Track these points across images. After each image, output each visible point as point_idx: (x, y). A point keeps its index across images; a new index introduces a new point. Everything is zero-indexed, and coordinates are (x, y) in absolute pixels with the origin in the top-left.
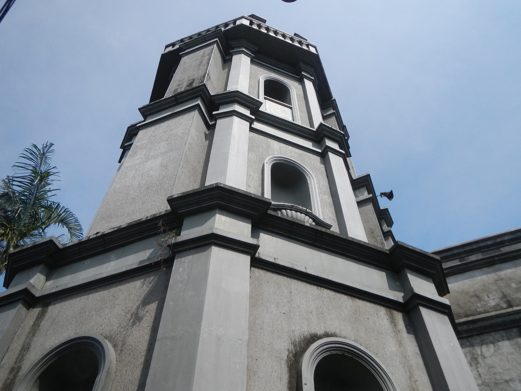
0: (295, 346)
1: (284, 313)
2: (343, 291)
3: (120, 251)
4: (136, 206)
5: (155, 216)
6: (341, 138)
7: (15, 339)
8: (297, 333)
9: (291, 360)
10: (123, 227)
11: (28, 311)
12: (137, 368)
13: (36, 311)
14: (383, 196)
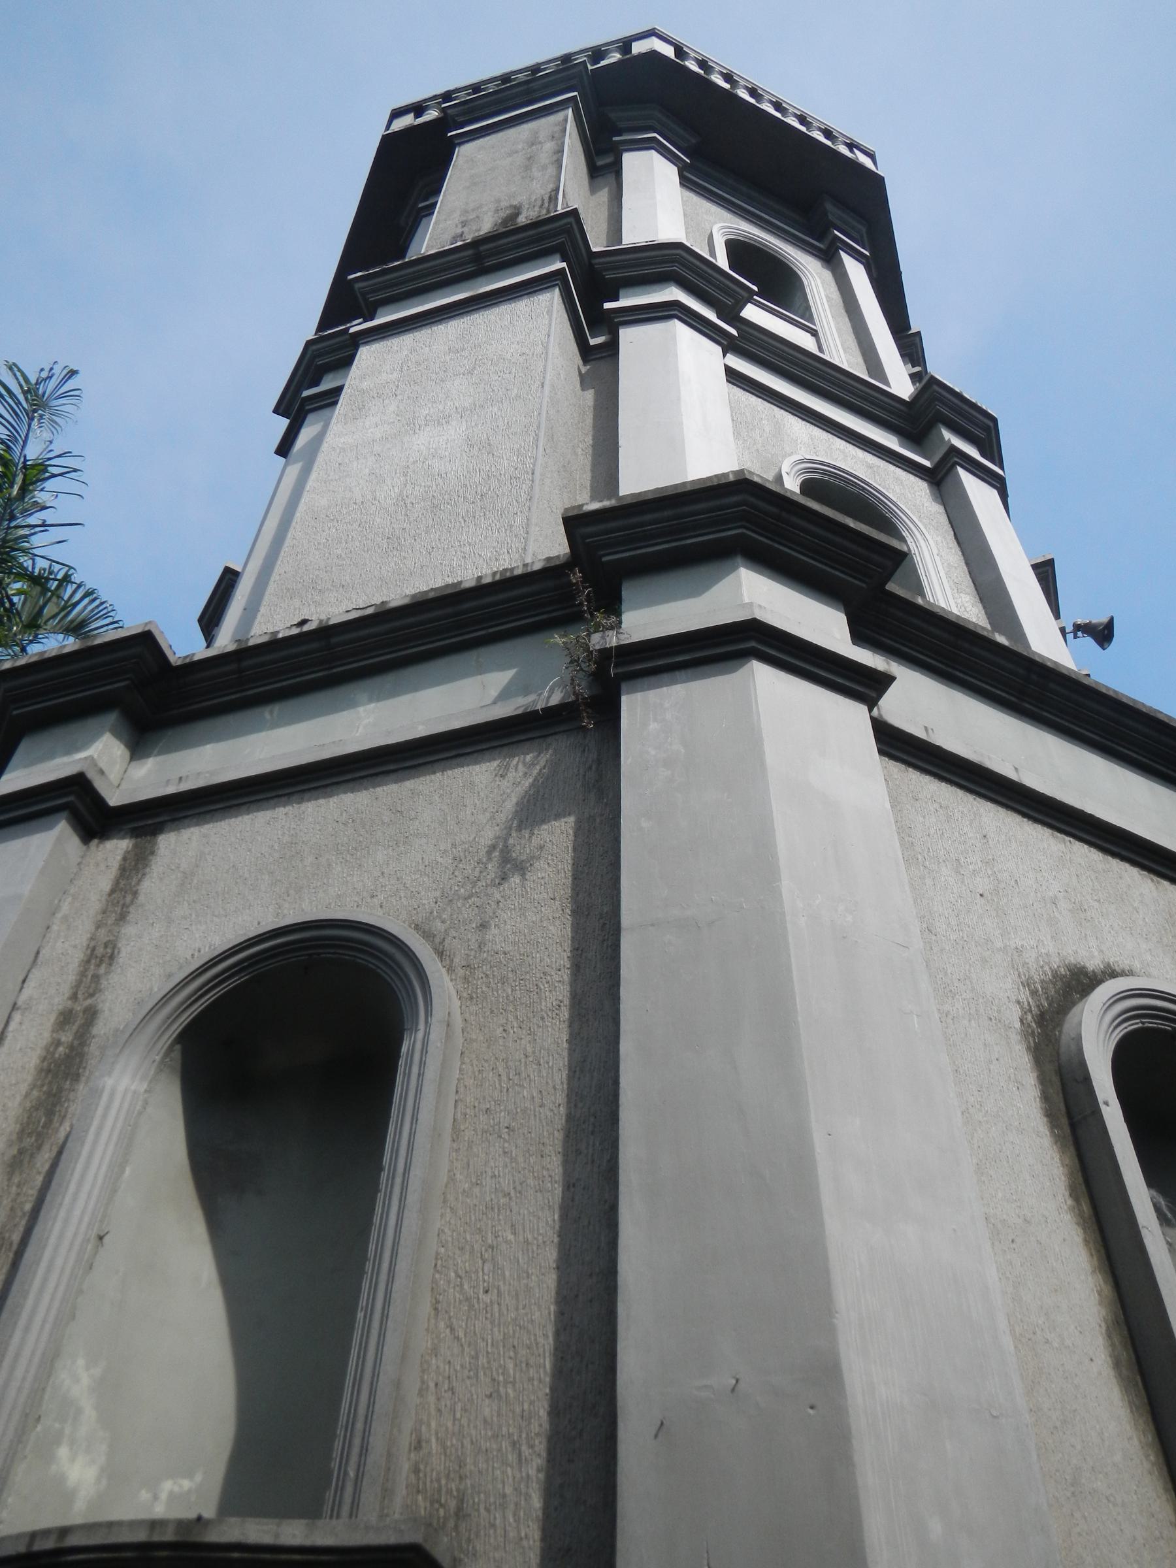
0: (1034, 993)
1: (981, 895)
2: (1124, 853)
3: (388, 680)
4: (405, 558)
5: (508, 574)
6: (987, 429)
7: (55, 928)
8: (1030, 957)
9: (1033, 1032)
10: (393, 604)
11: (84, 848)
12: (543, 1018)
13: (117, 848)
14: (1080, 634)
